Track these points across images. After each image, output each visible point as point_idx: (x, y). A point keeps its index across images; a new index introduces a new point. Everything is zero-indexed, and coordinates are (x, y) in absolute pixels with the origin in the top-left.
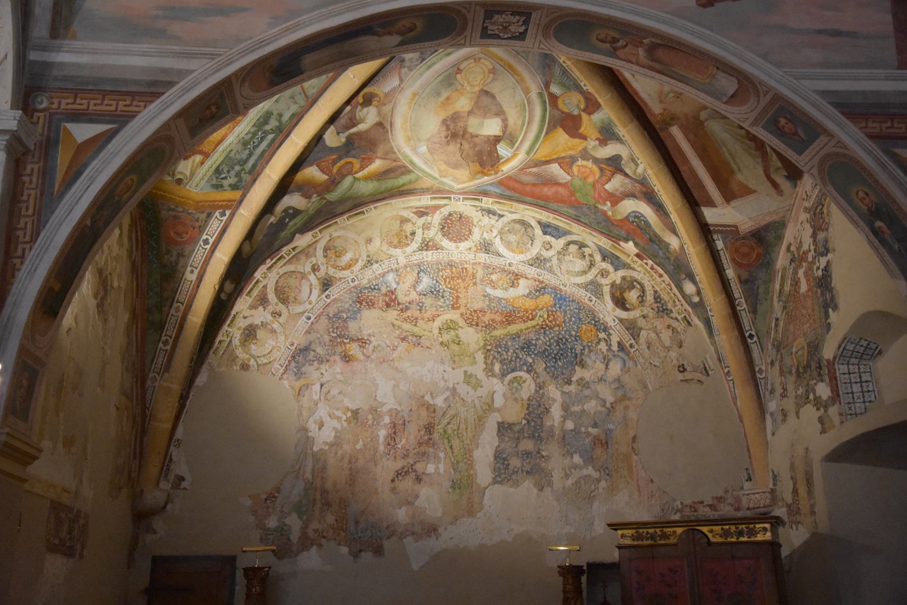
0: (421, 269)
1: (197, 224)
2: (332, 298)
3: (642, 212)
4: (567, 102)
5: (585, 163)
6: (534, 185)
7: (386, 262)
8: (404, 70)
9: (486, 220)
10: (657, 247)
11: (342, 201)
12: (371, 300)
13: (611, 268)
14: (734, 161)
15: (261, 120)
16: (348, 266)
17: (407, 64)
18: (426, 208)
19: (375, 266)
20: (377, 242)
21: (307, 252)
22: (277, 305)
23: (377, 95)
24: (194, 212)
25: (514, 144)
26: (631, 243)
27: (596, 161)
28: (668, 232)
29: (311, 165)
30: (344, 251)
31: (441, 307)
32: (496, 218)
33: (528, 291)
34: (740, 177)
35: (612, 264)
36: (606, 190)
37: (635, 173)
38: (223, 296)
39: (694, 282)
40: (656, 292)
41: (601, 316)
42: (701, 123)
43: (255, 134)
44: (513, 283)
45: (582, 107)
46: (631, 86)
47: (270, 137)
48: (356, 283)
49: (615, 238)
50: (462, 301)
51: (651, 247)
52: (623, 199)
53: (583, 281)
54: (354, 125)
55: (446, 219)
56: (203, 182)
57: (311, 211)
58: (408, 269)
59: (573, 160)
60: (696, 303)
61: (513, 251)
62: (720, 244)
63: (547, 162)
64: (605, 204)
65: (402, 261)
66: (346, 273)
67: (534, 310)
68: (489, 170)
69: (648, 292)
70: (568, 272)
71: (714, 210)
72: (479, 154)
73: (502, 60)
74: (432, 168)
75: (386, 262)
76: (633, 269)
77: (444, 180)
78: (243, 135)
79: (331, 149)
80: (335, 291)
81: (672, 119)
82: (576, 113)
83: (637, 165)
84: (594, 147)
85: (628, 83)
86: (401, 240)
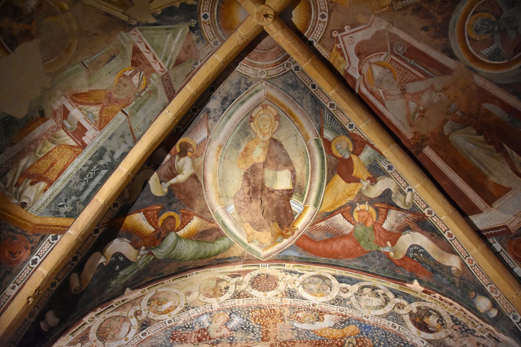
0: (232, 312)
1: (31, 245)
2: (148, 335)
3: (419, 244)
4: (338, 147)
5: (362, 207)
6: (326, 241)
7: (201, 308)
8: (211, 121)
9: (289, 277)
10: (439, 276)
11: (169, 260)
12: (184, 337)
13: (405, 302)
14: (483, 166)
15: (97, 154)
16: (168, 311)
17: (212, 115)
18: (239, 272)
19: (191, 311)
20: (195, 295)
21: (133, 303)
22: (95, 341)
23: (191, 146)
24: (31, 234)
25: (303, 196)
26: (416, 282)
27: (371, 202)
28: (446, 254)
29: (139, 212)
30: (167, 301)
31: (251, 340)
32: (298, 275)
33: (333, 323)
34: (493, 179)
35: (404, 298)
36: (384, 230)
37: (405, 203)
38: (42, 325)
39: (486, 295)
40: (452, 317)
41: (409, 339)
42: (447, 137)
43: (91, 167)
44: (318, 318)
45: (351, 149)
46: (385, 117)
47: (104, 172)
48: (173, 323)
49: (402, 281)
50: (272, 335)
51: (435, 276)
52: (400, 235)
53: (382, 313)
54: (174, 176)
55: (255, 278)
56: (43, 208)
57: (141, 265)
58: (221, 312)
59: (352, 205)
60: (494, 318)
61: (315, 295)
62: (498, 247)
63: (332, 214)
64: (386, 245)
65: (216, 306)
66: (166, 317)
67: (342, 338)
68: (287, 231)
69: (445, 318)
70: (367, 307)
71: (481, 216)
72: (277, 211)
73: (284, 107)
74: (241, 232)
75: (201, 308)
76: (425, 301)
77: (253, 246)
78: (81, 167)
79: (156, 198)
80: (151, 331)
81: (423, 140)
82: (347, 157)
83: (405, 195)
84: (367, 188)
85: (382, 114)
86: (216, 292)
